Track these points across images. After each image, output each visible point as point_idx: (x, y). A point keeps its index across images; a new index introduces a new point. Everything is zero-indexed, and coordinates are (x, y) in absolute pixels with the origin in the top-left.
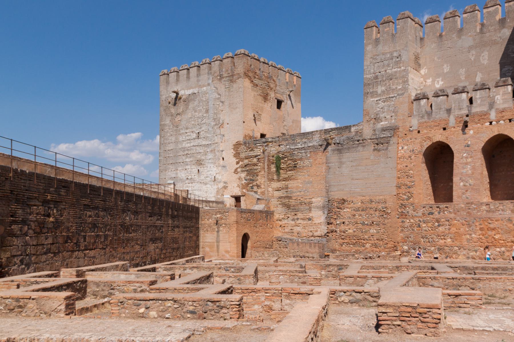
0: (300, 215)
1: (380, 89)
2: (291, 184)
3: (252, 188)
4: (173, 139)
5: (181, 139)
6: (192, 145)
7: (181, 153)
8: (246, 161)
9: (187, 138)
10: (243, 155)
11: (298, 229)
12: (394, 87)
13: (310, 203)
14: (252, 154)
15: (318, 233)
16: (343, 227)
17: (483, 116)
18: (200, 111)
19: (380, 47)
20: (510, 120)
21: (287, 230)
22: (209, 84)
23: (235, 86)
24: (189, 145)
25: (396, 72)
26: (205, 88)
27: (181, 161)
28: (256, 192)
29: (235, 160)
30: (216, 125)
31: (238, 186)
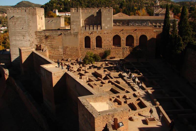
0: (55, 50)
1: (75, 24)
2: (52, 42)
3: (41, 43)
4: (14, 29)
5: (16, 29)
6: (21, 31)
7: (17, 33)
8: (39, 36)
9: (19, 29)
10: (38, 35)
11: (55, 53)
12: (78, 24)
13: (58, 47)
14: (40, 34)
15: (61, 54)
16: (67, 53)
17: (96, 32)
18: (23, 22)
19: (74, 14)
20: (101, 33)
21: (52, 53)
22: (25, 15)
23: (34, 17)
24: (19, 31)
25: (78, 20)
26: (24, 16)
27: (17, 35)
28: (42, 44)
29: (35, 36)
30: (29, 26)
31: (37, 42)
